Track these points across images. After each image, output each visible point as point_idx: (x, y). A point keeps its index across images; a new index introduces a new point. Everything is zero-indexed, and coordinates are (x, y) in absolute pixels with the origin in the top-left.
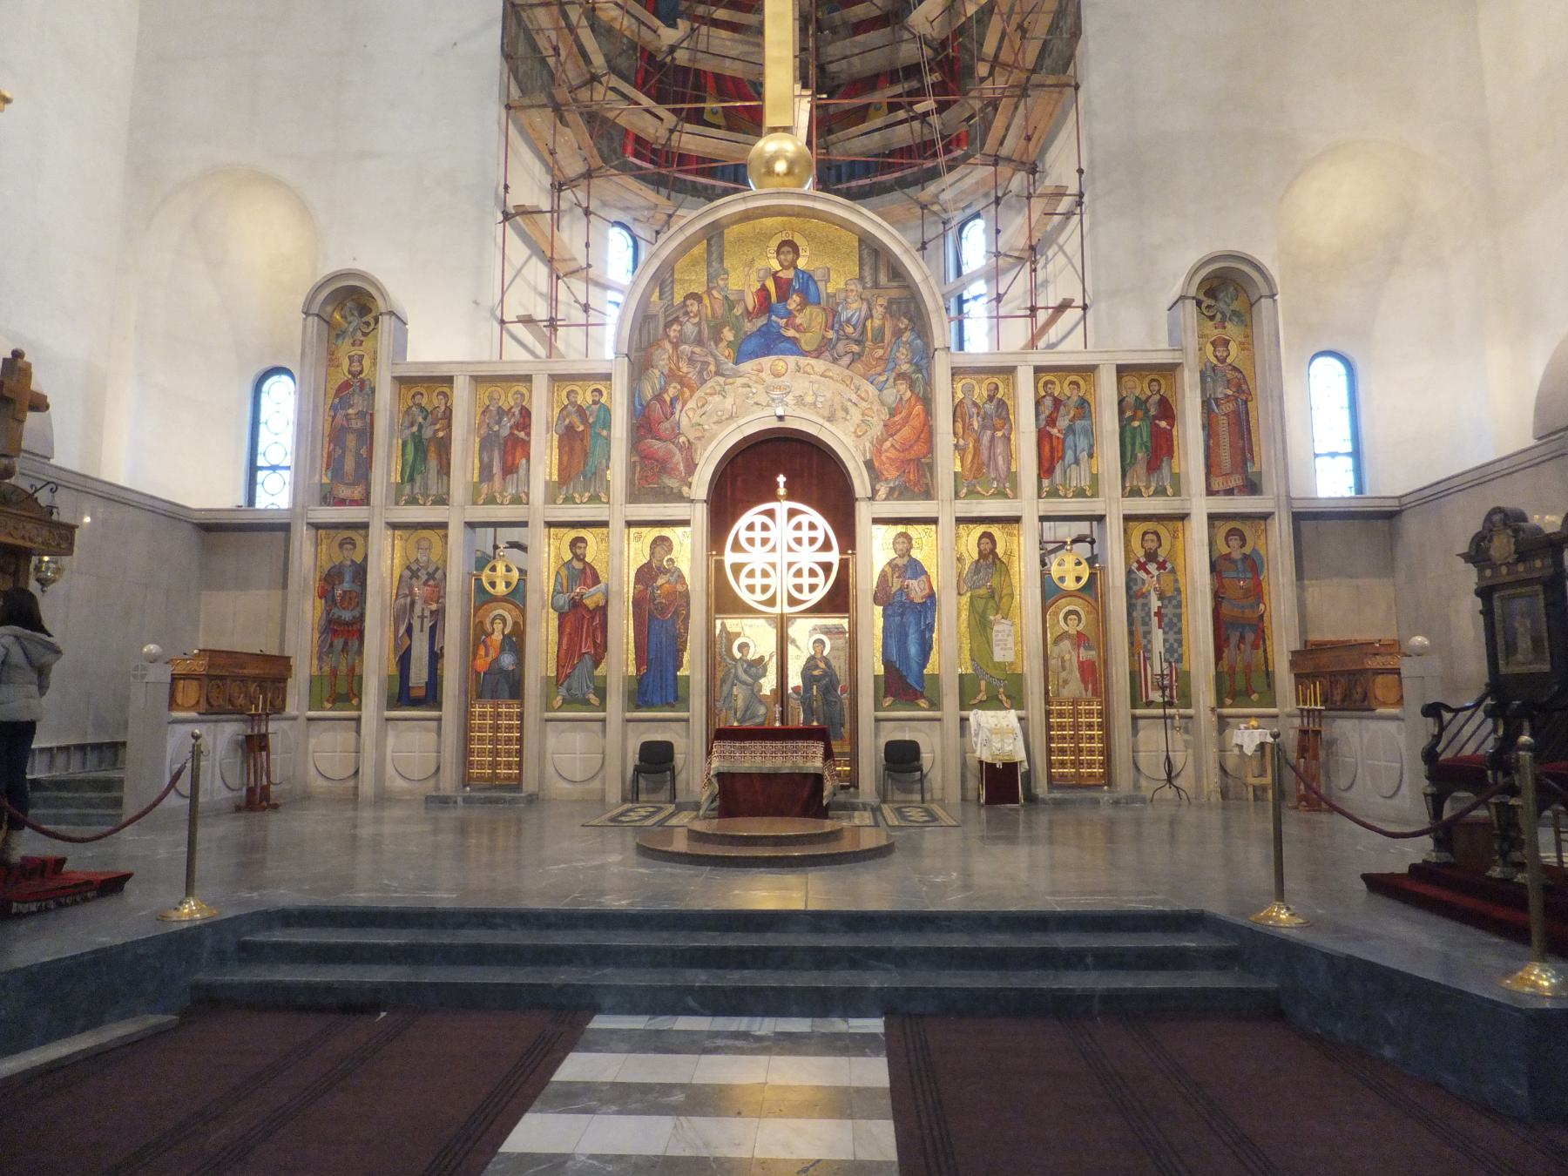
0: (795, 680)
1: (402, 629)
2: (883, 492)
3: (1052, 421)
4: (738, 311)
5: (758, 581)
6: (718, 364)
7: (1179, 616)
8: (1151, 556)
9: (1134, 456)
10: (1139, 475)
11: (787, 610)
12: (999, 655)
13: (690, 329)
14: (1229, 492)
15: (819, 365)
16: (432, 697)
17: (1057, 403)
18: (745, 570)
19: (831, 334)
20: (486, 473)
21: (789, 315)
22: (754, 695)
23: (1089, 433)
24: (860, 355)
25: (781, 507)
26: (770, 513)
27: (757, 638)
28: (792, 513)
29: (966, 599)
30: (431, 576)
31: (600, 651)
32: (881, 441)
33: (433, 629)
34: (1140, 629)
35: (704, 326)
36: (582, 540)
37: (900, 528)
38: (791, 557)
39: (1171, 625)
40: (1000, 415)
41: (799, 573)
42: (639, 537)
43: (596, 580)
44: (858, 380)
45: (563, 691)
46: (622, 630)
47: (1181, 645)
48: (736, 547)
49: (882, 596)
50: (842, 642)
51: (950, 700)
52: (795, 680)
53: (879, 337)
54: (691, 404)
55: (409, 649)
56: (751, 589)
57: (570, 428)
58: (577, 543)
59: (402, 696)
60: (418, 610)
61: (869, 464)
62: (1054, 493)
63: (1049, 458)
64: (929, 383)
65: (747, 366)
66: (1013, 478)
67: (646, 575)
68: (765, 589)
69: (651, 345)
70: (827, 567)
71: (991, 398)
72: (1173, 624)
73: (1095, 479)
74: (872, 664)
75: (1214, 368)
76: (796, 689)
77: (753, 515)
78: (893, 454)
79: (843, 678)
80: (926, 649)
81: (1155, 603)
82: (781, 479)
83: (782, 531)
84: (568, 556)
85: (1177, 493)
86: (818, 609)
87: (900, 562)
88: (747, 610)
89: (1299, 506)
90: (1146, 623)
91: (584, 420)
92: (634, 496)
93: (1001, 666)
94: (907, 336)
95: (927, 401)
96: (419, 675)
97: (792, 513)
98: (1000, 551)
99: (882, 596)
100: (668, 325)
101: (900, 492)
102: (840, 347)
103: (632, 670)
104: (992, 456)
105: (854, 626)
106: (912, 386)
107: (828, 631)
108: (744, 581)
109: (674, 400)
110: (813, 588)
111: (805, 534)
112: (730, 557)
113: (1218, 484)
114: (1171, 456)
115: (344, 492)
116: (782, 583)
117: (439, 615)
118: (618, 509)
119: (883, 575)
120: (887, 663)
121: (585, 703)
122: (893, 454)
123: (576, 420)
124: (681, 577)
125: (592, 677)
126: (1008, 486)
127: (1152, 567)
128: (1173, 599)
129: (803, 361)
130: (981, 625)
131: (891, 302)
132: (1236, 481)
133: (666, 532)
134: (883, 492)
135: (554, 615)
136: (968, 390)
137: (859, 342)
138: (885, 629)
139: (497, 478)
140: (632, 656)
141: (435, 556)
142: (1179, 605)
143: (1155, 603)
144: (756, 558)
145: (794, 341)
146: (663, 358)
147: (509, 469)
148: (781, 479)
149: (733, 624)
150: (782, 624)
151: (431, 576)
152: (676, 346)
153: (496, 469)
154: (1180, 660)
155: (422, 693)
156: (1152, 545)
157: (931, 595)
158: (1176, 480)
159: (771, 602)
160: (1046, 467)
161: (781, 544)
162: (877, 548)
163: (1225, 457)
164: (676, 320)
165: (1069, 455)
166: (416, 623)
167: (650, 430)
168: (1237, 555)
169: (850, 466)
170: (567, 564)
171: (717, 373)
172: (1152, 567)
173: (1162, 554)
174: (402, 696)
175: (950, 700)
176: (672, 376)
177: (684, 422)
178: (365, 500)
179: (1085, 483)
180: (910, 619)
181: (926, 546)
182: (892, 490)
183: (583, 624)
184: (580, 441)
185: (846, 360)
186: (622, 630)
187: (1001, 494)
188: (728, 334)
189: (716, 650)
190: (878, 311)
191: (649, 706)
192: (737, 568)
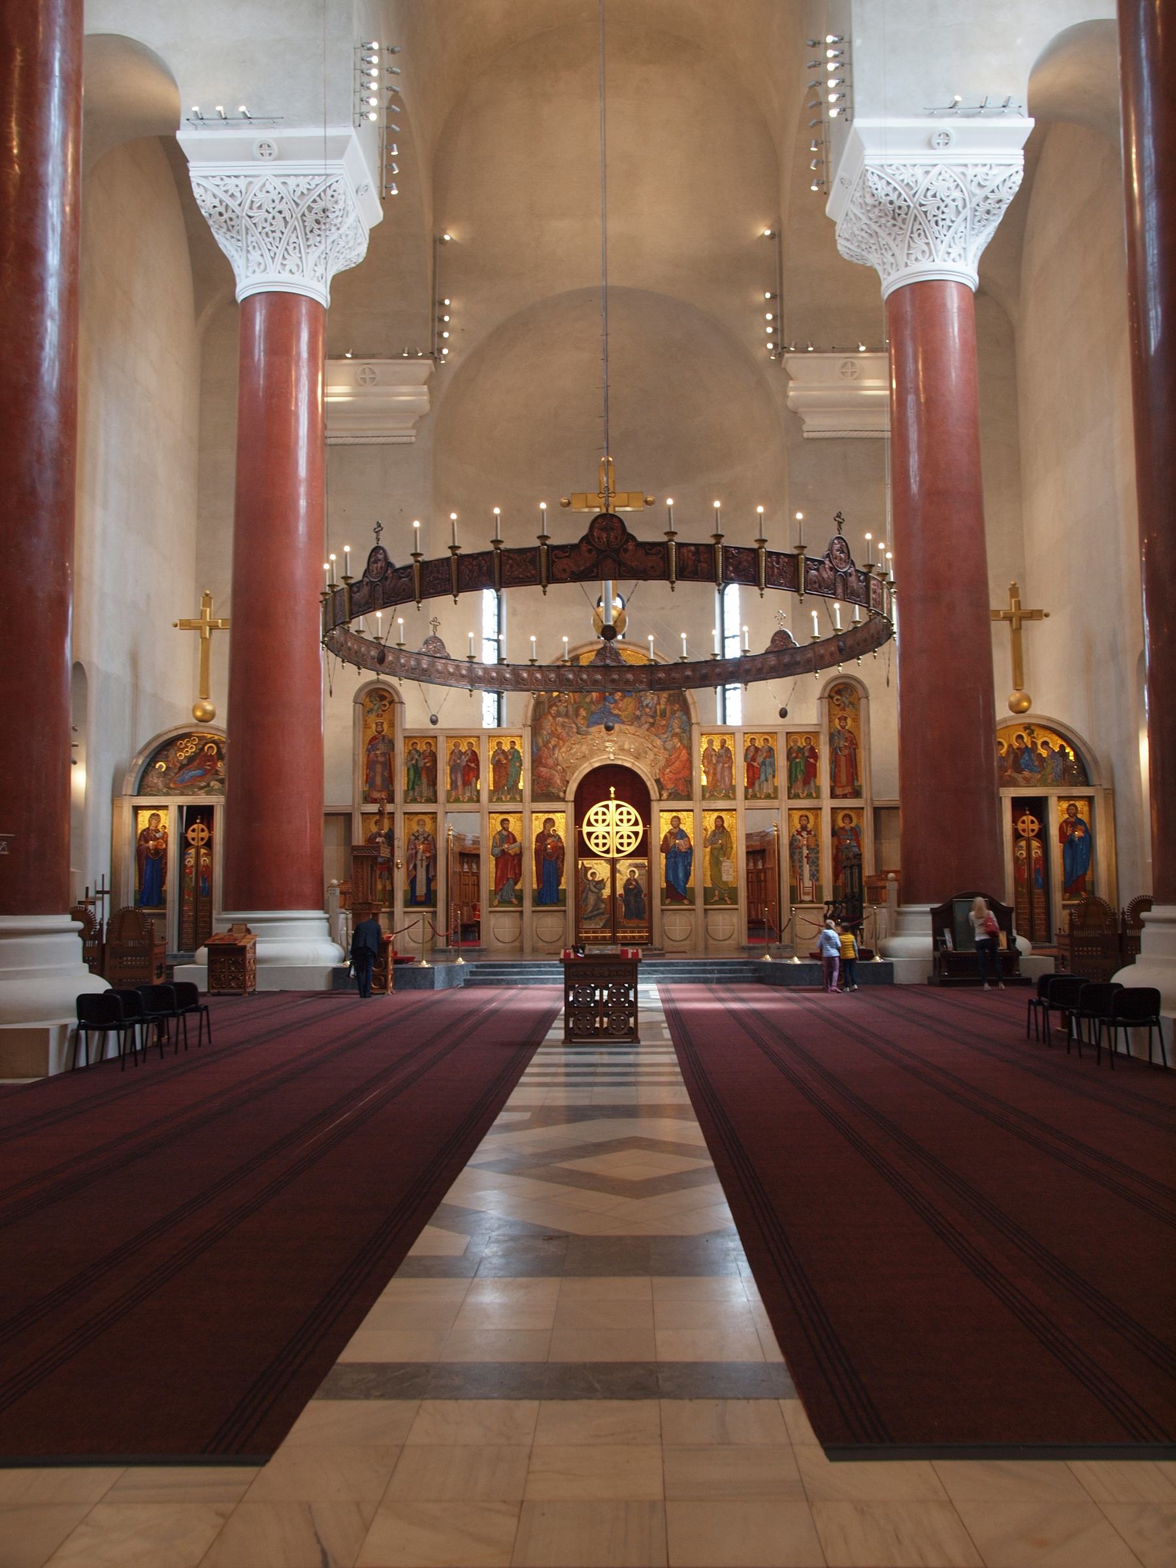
0: (620, 891)
1: (411, 867)
2: (665, 795)
3: (754, 759)
4: (588, 700)
5: (600, 841)
6: (578, 728)
7: (818, 858)
8: (804, 828)
9: (796, 777)
10: (798, 788)
11: (616, 855)
12: (725, 878)
13: (562, 709)
14: (845, 796)
15: (632, 729)
16: (430, 899)
17: (757, 749)
18: (594, 836)
19: (638, 713)
20: (454, 783)
21: (616, 702)
22: (599, 899)
23: (773, 765)
24: (652, 725)
25: (612, 804)
26: (607, 807)
27: (601, 870)
28: (618, 806)
29: (708, 849)
30: (426, 839)
31: (518, 876)
32: (665, 767)
33: (428, 866)
34: (798, 864)
35: (570, 709)
36: (507, 820)
37: (674, 814)
38: (618, 829)
39: (814, 863)
40: (726, 755)
41: (622, 837)
42: (537, 818)
43: (515, 840)
44: (653, 737)
45: (498, 897)
46: (530, 865)
47: (818, 871)
48: (589, 824)
49: (665, 848)
50: (644, 872)
51: (699, 900)
52: (620, 891)
53: (663, 714)
54: (563, 749)
55: (415, 877)
56: (597, 845)
57: (499, 761)
58: (504, 821)
59: (412, 900)
60: (419, 857)
61: (658, 781)
62: (754, 797)
63: (753, 774)
64: (690, 739)
65: (593, 729)
66: (733, 788)
67: (541, 838)
68: (604, 845)
69: (541, 717)
70: (636, 834)
71: (722, 746)
72: (814, 862)
73: (776, 788)
74: (659, 882)
75: (839, 732)
76: (621, 895)
77: (597, 808)
78: (671, 775)
79: (645, 891)
80: (687, 875)
81: (805, 852)
82: (612, 789)
83: (613, 815)
84: (499, 828)
85: (818, 797)
86: (631, 855)
87: (675, 831)
88: (595, 856)
89: (877, 804)
90: (800, 861)
91: (506, 758)
92: (535, 798)
93: (726, 883)
94: (678, 714)
95: (689, 748)
96: (421, 890)
97: (618, 806)
98: (726, 825)
99: (665, 848)
100: (550, 707)
101: (674, 796)
102: (643, 719)
103: (535, 886)
104: (723, 777)
105: (650, 862)
106: (680, 741)
107: (636, 866)
108: (593, 841)
109: (554, 747)
110: (629, 844)
111: (625, 817)
112: (586, 829)
113: (839, 791)
114: (815, 776)
115: (376, 795)
116: (613, 842)
117: (432, 860)
118: (528, 805)
119: (666, 837)
120: (667, 881)
121: (510, 903)
122: (671, 775)
123: (502, 757)
124: (560, 838)
125: (514, 890)
126: (730, 794)
127: (804, 834)
128: (815, 849)
129: (624, 727)
130: (716, 863)
131: (670, 695)
132: (848, 790)
133: (551, 816)
134: (665, 795)
135: (493, 858)
136: (710, 742)
137: (652, 717)
138: (667, 865)
139: (460, 788)
140: (535, 879)
141: (428, 827)
142: (818, 852)
143: (805, 852)
144: (599, 829)
145: (618, 716)
146: (548, 724)
147: (466, 783)
148: (612, 789)
149: (588, 863)
150: (613, 862)
151: (426, 839)
152: (554, 718)
153: (460, 783)
154: (817, 880)
155: (423, 899)
156: (805, 823)
157: (691, 848)
158: (818, 789)
159: (607, 852)
160: (751, 783)
161: (612, 822)
162: (663, 824)
163: (843, 778)
164: (555, 704)
165: (763, 777)
166: (419, 863)
167: (541, 762)
168: (847, 827)
169: (648, 784)
170: (499, 833)
171: (578, 733)
172: (804, 834)
173: (810, 826)
174: (412, 900)
175: (699, 900)
176: (553, 734)
177: (560, 758)
178: (391, 800)
179: (771, 791)
180: (680, 860)
181: (687, 825)
182: (670, 794)
183: (509, 863)
184: (505, 764)
185: (647, 726)
186: (530, 865)
187: (727, 797)
188: (583, 713)
189: (580, 875)
190: (663, 700)
191: (545, 904)
192: (589, 834)
